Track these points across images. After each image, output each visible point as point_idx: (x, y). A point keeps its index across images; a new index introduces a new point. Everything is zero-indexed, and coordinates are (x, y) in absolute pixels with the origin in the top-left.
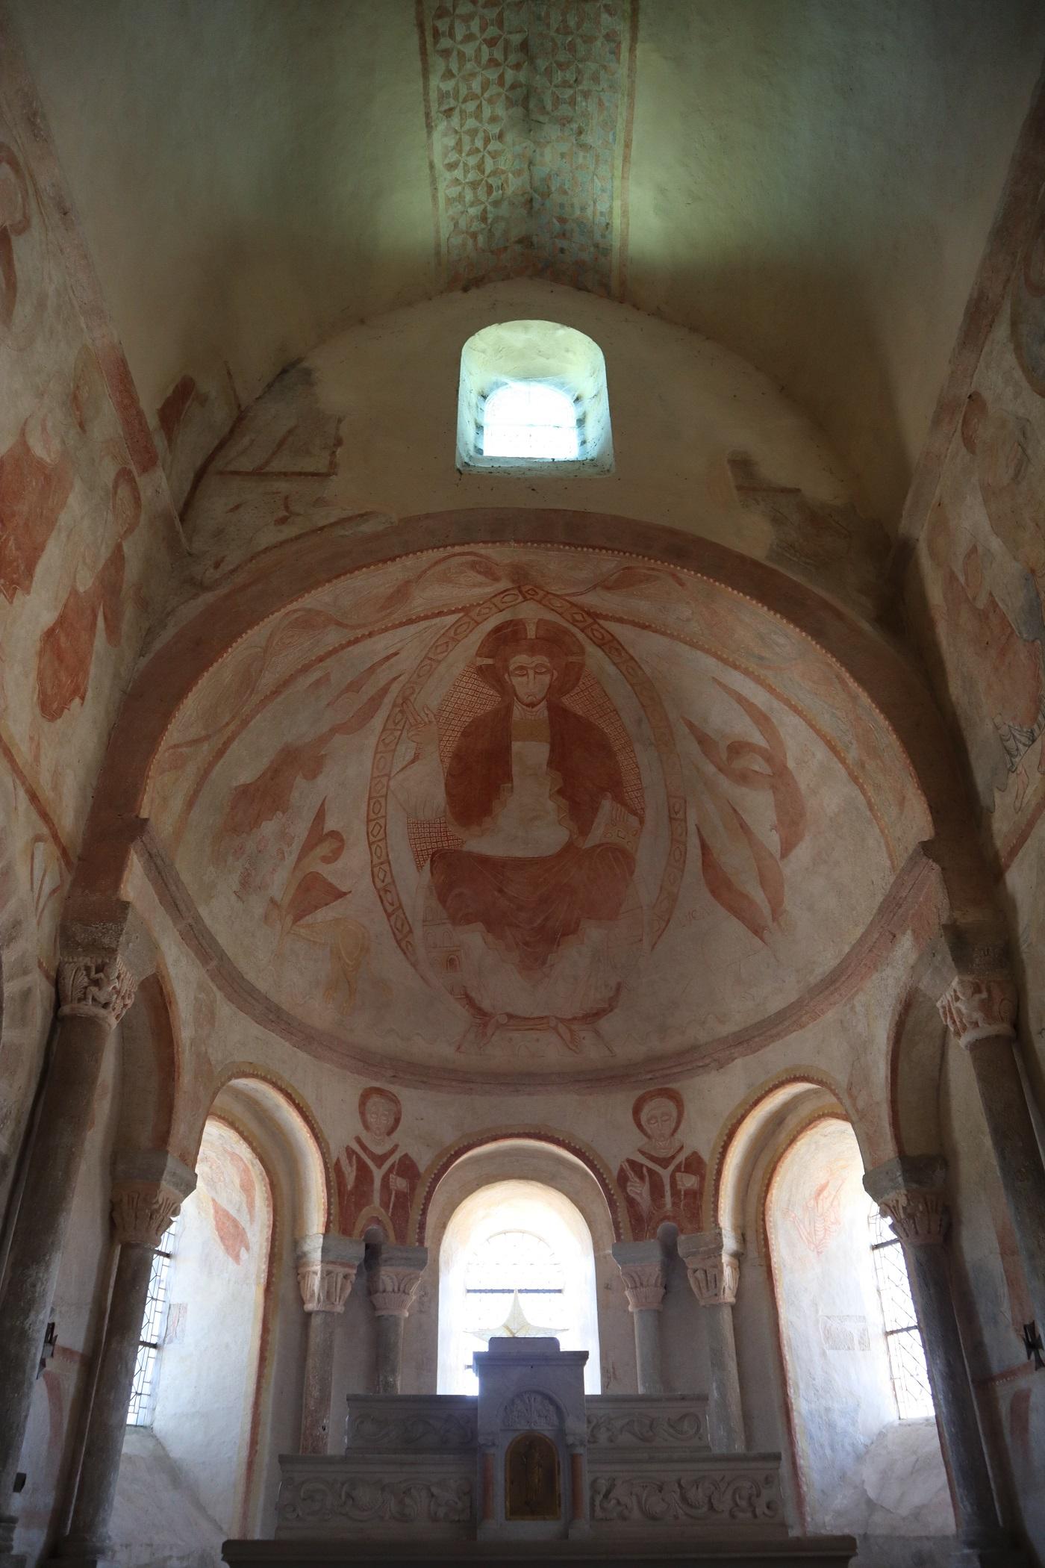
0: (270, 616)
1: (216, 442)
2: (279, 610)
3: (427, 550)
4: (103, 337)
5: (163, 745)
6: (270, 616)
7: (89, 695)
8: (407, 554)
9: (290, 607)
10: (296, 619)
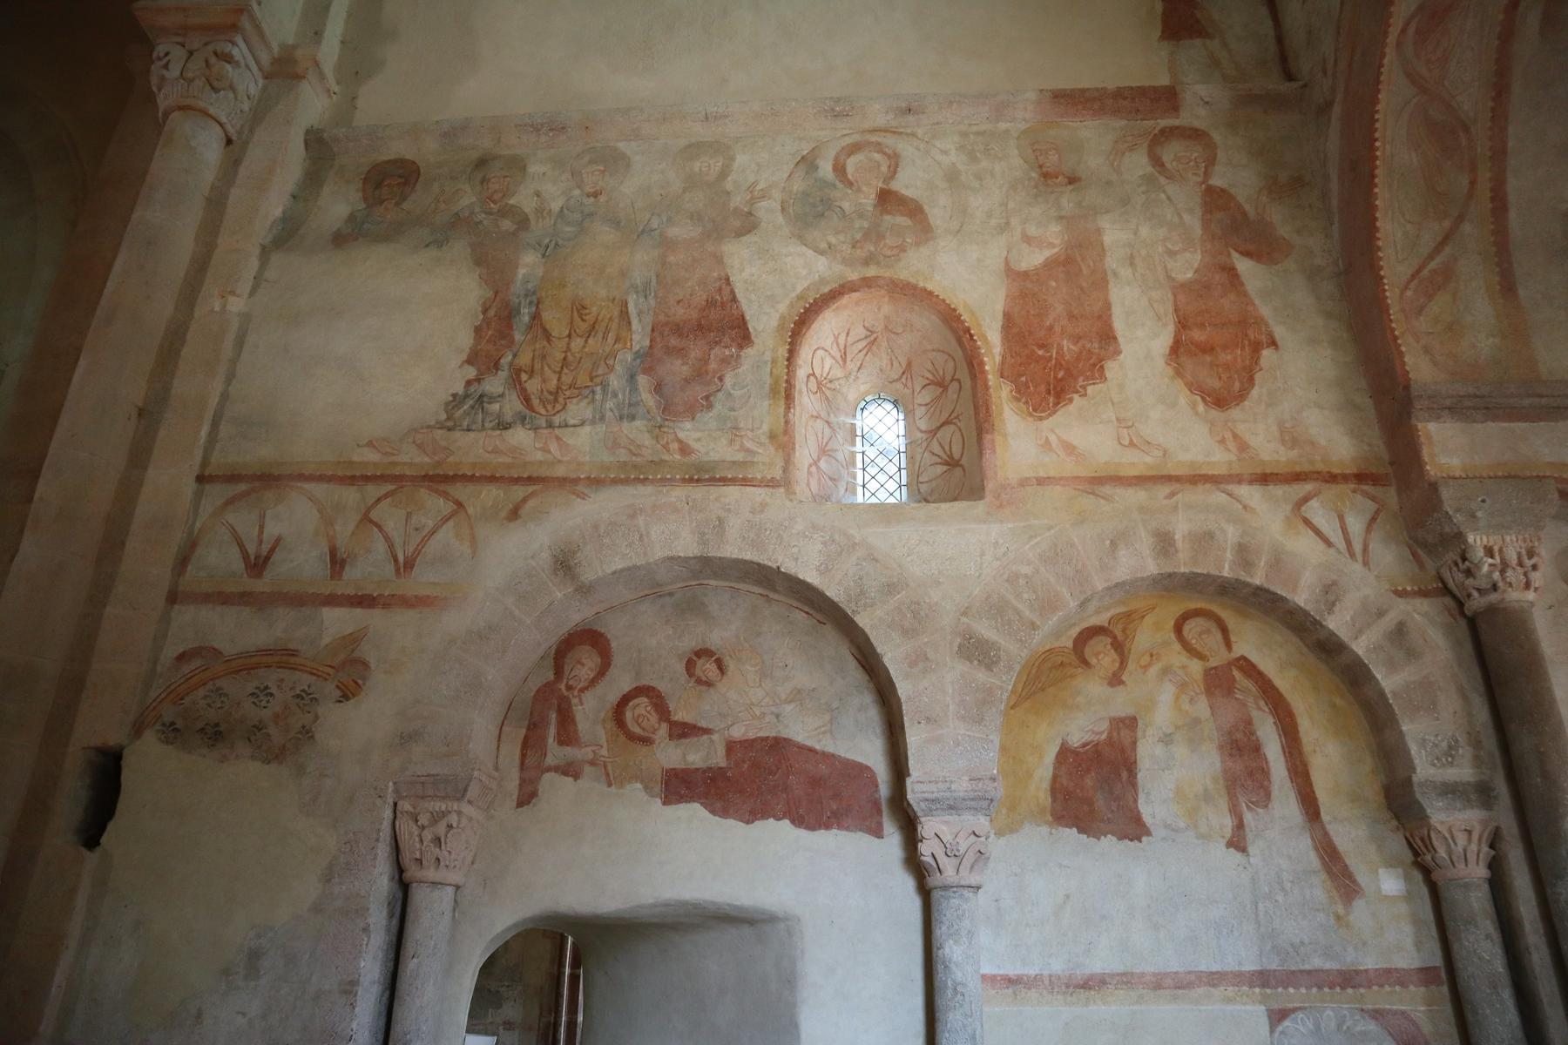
0: (1382, 70)
2: (1383, 56)
4: (1026, 109)
5: (1391, 295)
7: (1279, 332)
9: (1392, 39)
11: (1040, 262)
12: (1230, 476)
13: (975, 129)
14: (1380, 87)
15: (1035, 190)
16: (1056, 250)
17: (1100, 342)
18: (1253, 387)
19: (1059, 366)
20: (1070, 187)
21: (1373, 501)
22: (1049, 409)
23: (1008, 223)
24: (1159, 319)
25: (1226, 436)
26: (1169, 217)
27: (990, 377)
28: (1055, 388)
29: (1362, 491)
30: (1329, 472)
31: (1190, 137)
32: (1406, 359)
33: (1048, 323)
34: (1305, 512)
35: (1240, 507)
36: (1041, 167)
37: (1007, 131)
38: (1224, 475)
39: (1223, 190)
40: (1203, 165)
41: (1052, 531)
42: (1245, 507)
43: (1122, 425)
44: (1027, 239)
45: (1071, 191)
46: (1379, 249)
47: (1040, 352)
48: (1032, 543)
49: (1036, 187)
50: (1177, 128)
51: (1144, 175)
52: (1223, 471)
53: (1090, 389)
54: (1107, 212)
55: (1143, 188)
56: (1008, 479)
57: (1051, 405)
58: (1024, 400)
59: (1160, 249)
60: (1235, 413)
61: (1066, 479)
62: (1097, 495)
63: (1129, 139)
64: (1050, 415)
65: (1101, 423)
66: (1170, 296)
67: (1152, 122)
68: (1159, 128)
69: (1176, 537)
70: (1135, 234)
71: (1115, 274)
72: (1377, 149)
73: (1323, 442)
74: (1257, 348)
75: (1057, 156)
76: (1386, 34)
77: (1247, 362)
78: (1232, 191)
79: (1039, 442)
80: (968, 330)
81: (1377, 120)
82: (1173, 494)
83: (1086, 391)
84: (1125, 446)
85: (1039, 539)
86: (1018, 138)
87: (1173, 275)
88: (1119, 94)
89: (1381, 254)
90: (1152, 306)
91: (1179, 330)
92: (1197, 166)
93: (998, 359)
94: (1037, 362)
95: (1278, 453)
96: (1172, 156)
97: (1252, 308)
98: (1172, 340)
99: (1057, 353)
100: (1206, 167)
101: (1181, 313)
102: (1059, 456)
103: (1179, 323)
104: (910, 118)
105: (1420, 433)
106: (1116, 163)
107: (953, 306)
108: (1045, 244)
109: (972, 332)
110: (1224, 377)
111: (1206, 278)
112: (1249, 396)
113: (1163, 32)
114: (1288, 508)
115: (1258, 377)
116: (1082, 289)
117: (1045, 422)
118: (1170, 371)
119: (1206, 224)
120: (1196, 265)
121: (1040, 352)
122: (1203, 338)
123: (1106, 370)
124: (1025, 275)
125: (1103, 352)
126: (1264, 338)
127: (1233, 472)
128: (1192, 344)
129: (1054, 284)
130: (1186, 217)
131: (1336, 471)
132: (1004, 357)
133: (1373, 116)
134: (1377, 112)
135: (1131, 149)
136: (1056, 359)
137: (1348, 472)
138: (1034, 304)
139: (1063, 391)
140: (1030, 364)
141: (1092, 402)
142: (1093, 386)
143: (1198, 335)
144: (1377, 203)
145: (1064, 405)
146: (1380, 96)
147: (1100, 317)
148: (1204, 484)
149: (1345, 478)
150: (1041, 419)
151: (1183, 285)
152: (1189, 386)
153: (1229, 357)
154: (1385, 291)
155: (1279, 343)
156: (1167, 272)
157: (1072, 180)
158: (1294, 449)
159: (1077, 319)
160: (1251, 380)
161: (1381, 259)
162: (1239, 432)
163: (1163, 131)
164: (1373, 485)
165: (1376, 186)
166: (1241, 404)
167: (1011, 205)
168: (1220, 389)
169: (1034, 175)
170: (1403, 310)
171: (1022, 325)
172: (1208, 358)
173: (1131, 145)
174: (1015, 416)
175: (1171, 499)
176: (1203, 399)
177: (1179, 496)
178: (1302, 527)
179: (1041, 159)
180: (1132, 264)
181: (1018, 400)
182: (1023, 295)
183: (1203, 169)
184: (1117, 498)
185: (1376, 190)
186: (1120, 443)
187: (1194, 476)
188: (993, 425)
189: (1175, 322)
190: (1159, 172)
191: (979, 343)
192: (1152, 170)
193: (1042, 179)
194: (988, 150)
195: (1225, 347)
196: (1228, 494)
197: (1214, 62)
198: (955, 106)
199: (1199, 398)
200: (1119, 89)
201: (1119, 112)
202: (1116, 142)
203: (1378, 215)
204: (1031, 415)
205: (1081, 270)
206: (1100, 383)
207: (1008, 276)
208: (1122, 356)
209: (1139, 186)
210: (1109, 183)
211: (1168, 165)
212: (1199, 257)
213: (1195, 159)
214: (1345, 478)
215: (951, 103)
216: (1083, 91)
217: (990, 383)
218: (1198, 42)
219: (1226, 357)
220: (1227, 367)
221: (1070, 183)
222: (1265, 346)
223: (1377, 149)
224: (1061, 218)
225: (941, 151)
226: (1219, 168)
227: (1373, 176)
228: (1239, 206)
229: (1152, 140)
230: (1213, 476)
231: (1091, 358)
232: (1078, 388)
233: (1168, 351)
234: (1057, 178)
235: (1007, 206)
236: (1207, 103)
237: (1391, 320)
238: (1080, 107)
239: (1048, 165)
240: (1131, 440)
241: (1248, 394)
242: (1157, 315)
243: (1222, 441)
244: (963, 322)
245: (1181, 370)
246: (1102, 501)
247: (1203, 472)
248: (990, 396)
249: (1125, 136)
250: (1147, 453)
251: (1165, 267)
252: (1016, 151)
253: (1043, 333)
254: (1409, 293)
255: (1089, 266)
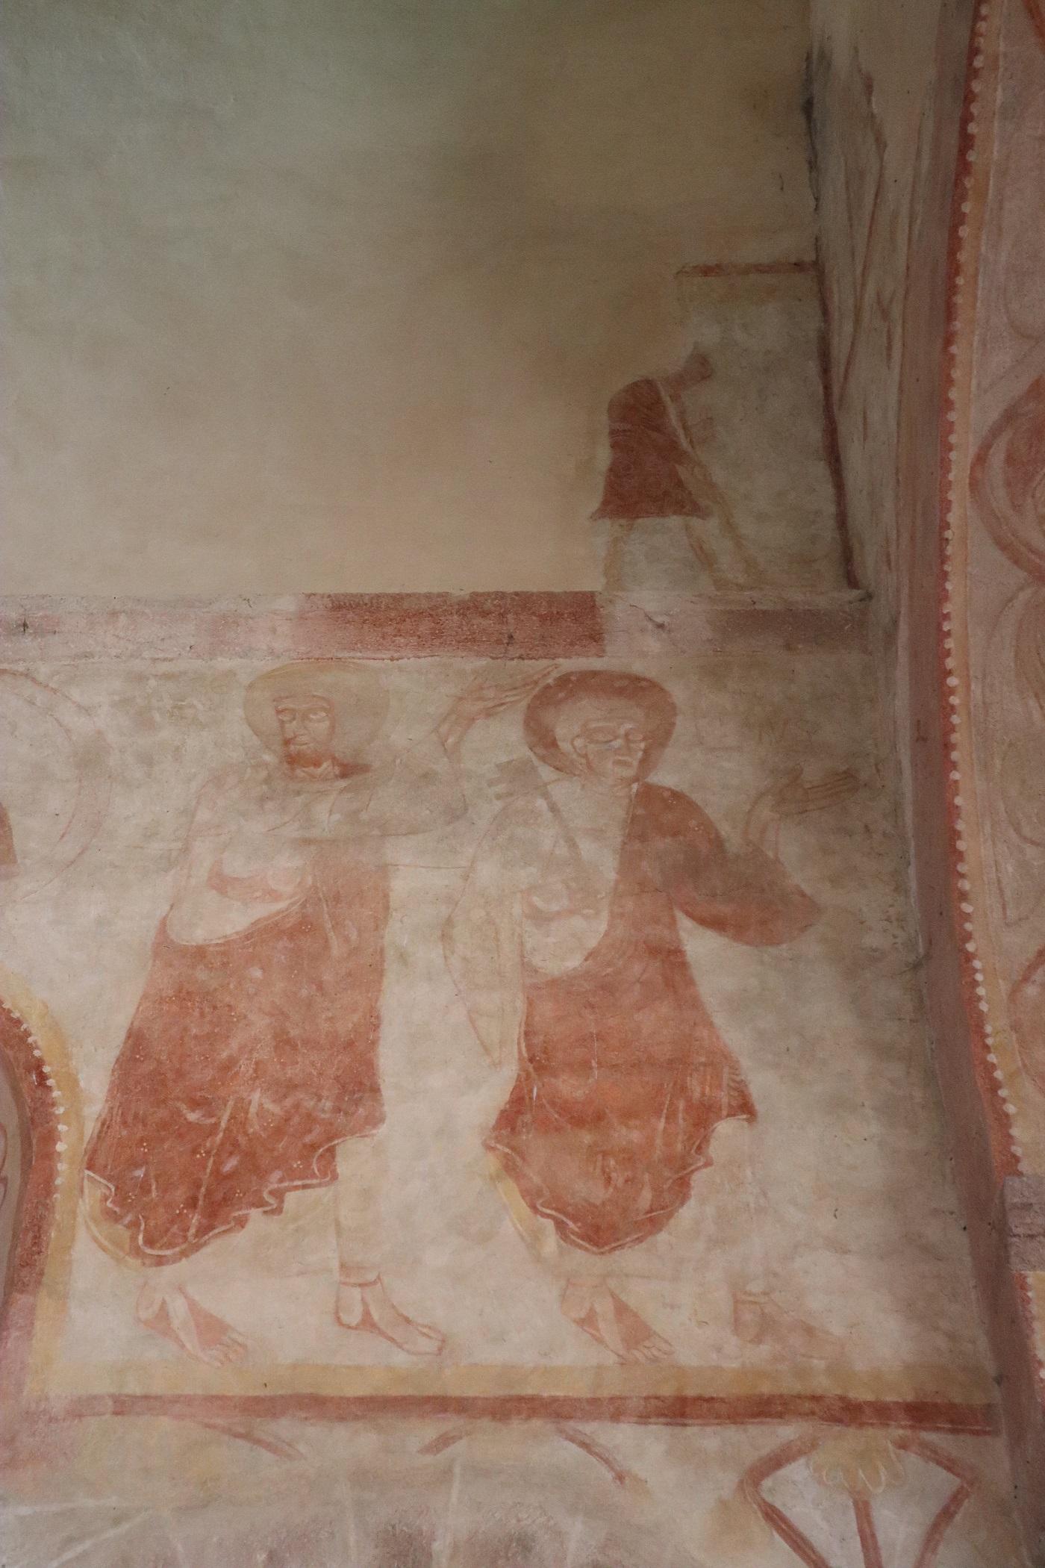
0: (948, 534)
1: (812, 368)
2: (946, 505)
3: (974, 34)
4: (274, 631)
6: (948, 534)
7: (760, 1083)
8: (969, 98)
9: (959, 472)
10: (1010, 459)
11: (239, 928)
12: (594, 1401)
13: (164, 668)
14: (947, 568)
15: (265, 787)
16: (281, 905)
17: (339, 1098)
18: (682, 1204)
19: (231, 1145)
20: (343, 783)
21: (949, 1469)
22: (185, 1238)
23: (186, 850)
24: (487, 1050)
25: (598, 1308)
26: (547, 844)
27: (62, 1167)
28: (209, 1193)
29: (924, 1445)
30: (842, 1398)
31: (621, 692)
32: (1015, 1132)
33: (224, 1055)
34: (771, 1490)
35: (609, 1476)
36: (287, 742)
37: (231, 673)
38: (579, 1400)
39: (676, 795)
40: (642, 745)
41: (125, 1527)
42: (620, 1477)
43: (352, 1280)
44: (221, 883)
45: (342, 791)
46: (963, 896)
47: (192, 1117)
48: (69, 1555)
49: (267, 780)
50: (595, 674)
51: (509, 763)
52: (579, 1388)
53: (291, 1198)
54: (413, 831)
55: (500, 788)
56: (47, 1399)
57: (193, 1231)
58: (129, 1218)
59: (517, 910)
60: (631, 1258)
61: (189, 1400)
62: (258, 1442)
63: (490, 693)
64: (184, 1254)
65: (301, 1273)
66: (520, 1004)
67: (543, 663)
68: (555, 674)
69: (436, 1546)
70: (466, 878)
71: (403, 957)
72: (952, 691)
73: (837, 1329)
74: (704, 1117)
75: (327, 723)
76: (945, 465)
77: (679, 1147)
78: (696, 797)
79: (144, 1315)
80: (37, 1066)
81: (948, 634)
82: (444, 1441)
83: (282, 1201)
84: (349, 1327)
85: (87, 1544)
86: (251, 687)
87: (537, 961)
88: (474, 606)
89: (967, 908)
90: (475, 1028)
91: (528, 1075)
92: (629, 749)
93: (91, 1128)
94: (180, 1136)
95: (719, 1350)
96: (577, 729)
97: (705, 1033)
98: (507, 1097)
99: (232, 1117)
100: (646, 751)
101: (538, 1040)
102: (183, 1346)
103: (531, 1060)
104: (27, 642)
105: (1030, 1294)
106: (451, 740)
107: (16, 1015)
108: (258, 894)
109: (46, 1069)
110: (619, 1179)
111: (609, 970)
112: (672, 1221)
113: (605, 503)
114: (728, 1480)
115: (699, 1180)
116: (320, 987)
117: (168, 1270)
118: (492, 1163)
119: (628, 862)
120: (592, 943)
121: (192, 1117)
122: (579, 1094)
123: (339, 1159)
124: (200, 954)
125: (341, 1119)
126: (724, 1098)
127: (605, 1393)
128: (553, 1104)
129: (257, 973)
130: (587, 848)
131: (862, 1394)
132: (105, 1125)
133: (939, 626)
134: (947, 617)
135: (489, 713)
136: (227, 1129)
137: (890, 1398)
138: (202, 1015)
139: (227, 1200)
140: (163, 1140)
141: (291, 1227)
142: (299, 1193)
143: (569, 1087)
144: (958, 801)
145: (224, 1232)
146: (949, 586)
147: (350, 1044)
148: (529, 1417)
149: (882, 1413)
150: (160, 1261)
151: (554, 983)
152: (533, 1198)
153: (636, 1136)
154: (975, 984)
155: (759, 1107)
156: (523, 957)
157: (347, 770)
158: (760, 1342)
159: (294, 1047)
160: (682, 1187)
161: (967, 917)
162: (632, 1302)
163: (564, 681)
164: (953, 1431)
165: (954, 766)
166: (650, 1239)
167: (203, 815)
168: (604, 1204)
169: (268, 757)
170: (1015, 1027)
171: (164, 1058)
172: (587, 1138)
173: (490, 704)
174: (101, 1254)
175: (438, 1451)
176: (560, 1226)
177: (459, 1448)
178: (759, 1529)
179: (292, 728)
180: (446, 937)
181: (116, 1218)
182: (183, 995)
183: (640, 754)
184: (302, 1448)
185: (955, 775)
186: (338, 1320)
187: (506, 1400)
188: (41, 1274)
189: (521, 1059)
190: (543, 759)
191: (56, 1094)
192: (530, 754)
193: (286, 766)
194: (180, 708)
195: (628, 1115)
196: (583, 1445)
197: (704, 559)
198: (123, 619)
199: (549, 1224)
200: (475, 595)
201: (474, 640)
202: (461, 699)
203: (960, 826)
204: (137, 1252)
205: (326, 945)
206: (320, 1185)
207: (156, 955)
208: (382, 1130)
209: (491, 784)
210: (428, 777)
211: (565, 746)
212: (603, 927)
213: (627, 735)
214: (882, 1413)
215: (114, 614)
216: (398, 598)
217: (58, 1181)
218: (674, 521)
219: (629, 1135)
220: (629, 1157)
221: (344, 775)
222: (724, 1113)
223: (952, 691)
224: (307, 842)
225: (79, 707)
226: (669, 752)
227: (948, 747)
228: (707, 825)
229: (536, 697)
230: (554, 1400)
231: (310, 1131)
232: (265, 1195)
233: (492, 1121)
234: (317, 764)
235: (193, 816)
236: (661, 626)
237: (987, 1048)
238: (389, 630)
239: (304, 739)
240: (367, 1313)
241: (670, 1216)
242: (482, 1043)
243: (588, 1321)
244: (31, 1048)
245: (518, 1160)
246: (267, 1456)
247: (529, 1391)
248: (49, 1208)
249: (482, 689)
250: (400, 1346)
251: (522, 944)
252: (240, 712)
253: (209, 1074)
254: (1031, 991)
255: (347, 940)
